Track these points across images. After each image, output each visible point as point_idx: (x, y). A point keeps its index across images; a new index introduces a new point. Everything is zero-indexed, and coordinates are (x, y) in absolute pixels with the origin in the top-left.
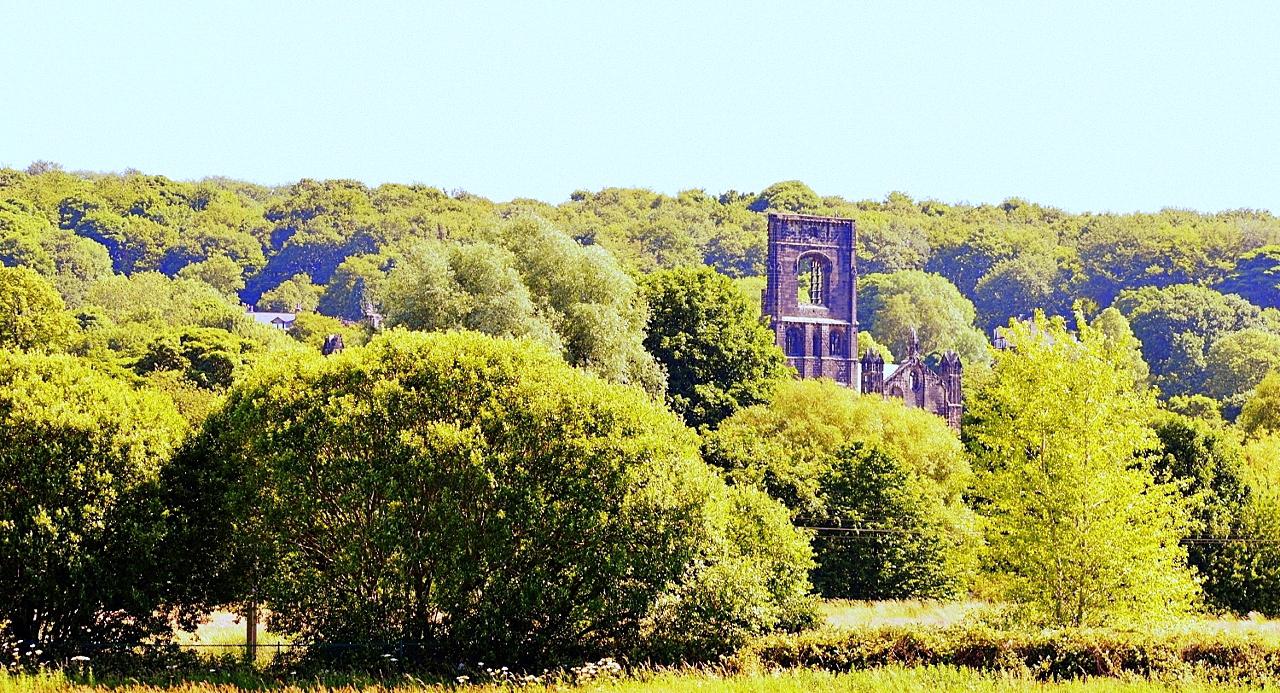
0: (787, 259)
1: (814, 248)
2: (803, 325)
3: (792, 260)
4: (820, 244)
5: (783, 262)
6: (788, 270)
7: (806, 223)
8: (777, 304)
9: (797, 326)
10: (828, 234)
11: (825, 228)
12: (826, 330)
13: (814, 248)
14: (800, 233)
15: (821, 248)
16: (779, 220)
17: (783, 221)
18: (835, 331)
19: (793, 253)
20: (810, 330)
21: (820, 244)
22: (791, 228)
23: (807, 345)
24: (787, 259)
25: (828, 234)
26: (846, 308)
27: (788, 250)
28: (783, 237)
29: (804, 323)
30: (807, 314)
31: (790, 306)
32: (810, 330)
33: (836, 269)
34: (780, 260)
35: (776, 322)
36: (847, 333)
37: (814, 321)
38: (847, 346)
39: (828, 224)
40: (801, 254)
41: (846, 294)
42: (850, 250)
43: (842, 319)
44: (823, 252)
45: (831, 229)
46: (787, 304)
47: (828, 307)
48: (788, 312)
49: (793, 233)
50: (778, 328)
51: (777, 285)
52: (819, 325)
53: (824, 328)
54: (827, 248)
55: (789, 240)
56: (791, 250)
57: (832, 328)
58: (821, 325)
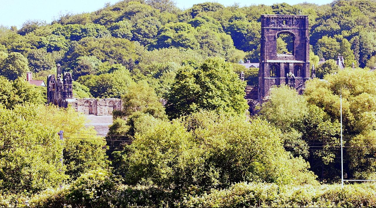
0: (270, 35)
1: (287, 29)
2: (279, 64)
3: (273, 35)
4: (288, 27)
5: (268, 36)
6: (271, 39)
7: (280, 18)
8: (264, 55)
9: (276, 64)
10: (292, 23)
11: (291, 20)
12: (291, 65)
13: (287, 29)
14: (277, 23)
15: (289, 29)
16: (265, 18)
17: (267, 18)
18: (297, 66)
19: (274, 32)
20: (282, 66)
21: (288, 27)
22: (272, 21)
23: (281, 72)
24: (270, 35)
25: (292, 23)
26: (303, 55)
27: (270, 31)
28: (268, 25)
29: (280, 63)
30: (282, 58)
31: (272, 55)
32: (282, 66)
33: (298, 38)
34: (266, 35)
35: (264, 63)
36: (304, 66)
37: (285, 61)
38: (304, 72)
39: (293, 18)
40: (278, 32)
41: (304, 49)
42: (305, 29)
43: (301, 60)
44: (291, 31)
45: (295, 21)
46: (270, 55)
47: (293, 55)
48: (271, 58)
49: (273, 23)
50: (265, 65)
51: (264, 46)
52: (288, 64)
53: (290, 65)
54: (293, 29)
55: (271, 26)
56: (273, 31)
57: (296, 65)
58: (289, 63)
